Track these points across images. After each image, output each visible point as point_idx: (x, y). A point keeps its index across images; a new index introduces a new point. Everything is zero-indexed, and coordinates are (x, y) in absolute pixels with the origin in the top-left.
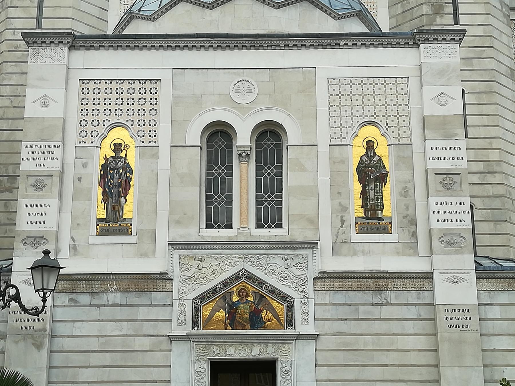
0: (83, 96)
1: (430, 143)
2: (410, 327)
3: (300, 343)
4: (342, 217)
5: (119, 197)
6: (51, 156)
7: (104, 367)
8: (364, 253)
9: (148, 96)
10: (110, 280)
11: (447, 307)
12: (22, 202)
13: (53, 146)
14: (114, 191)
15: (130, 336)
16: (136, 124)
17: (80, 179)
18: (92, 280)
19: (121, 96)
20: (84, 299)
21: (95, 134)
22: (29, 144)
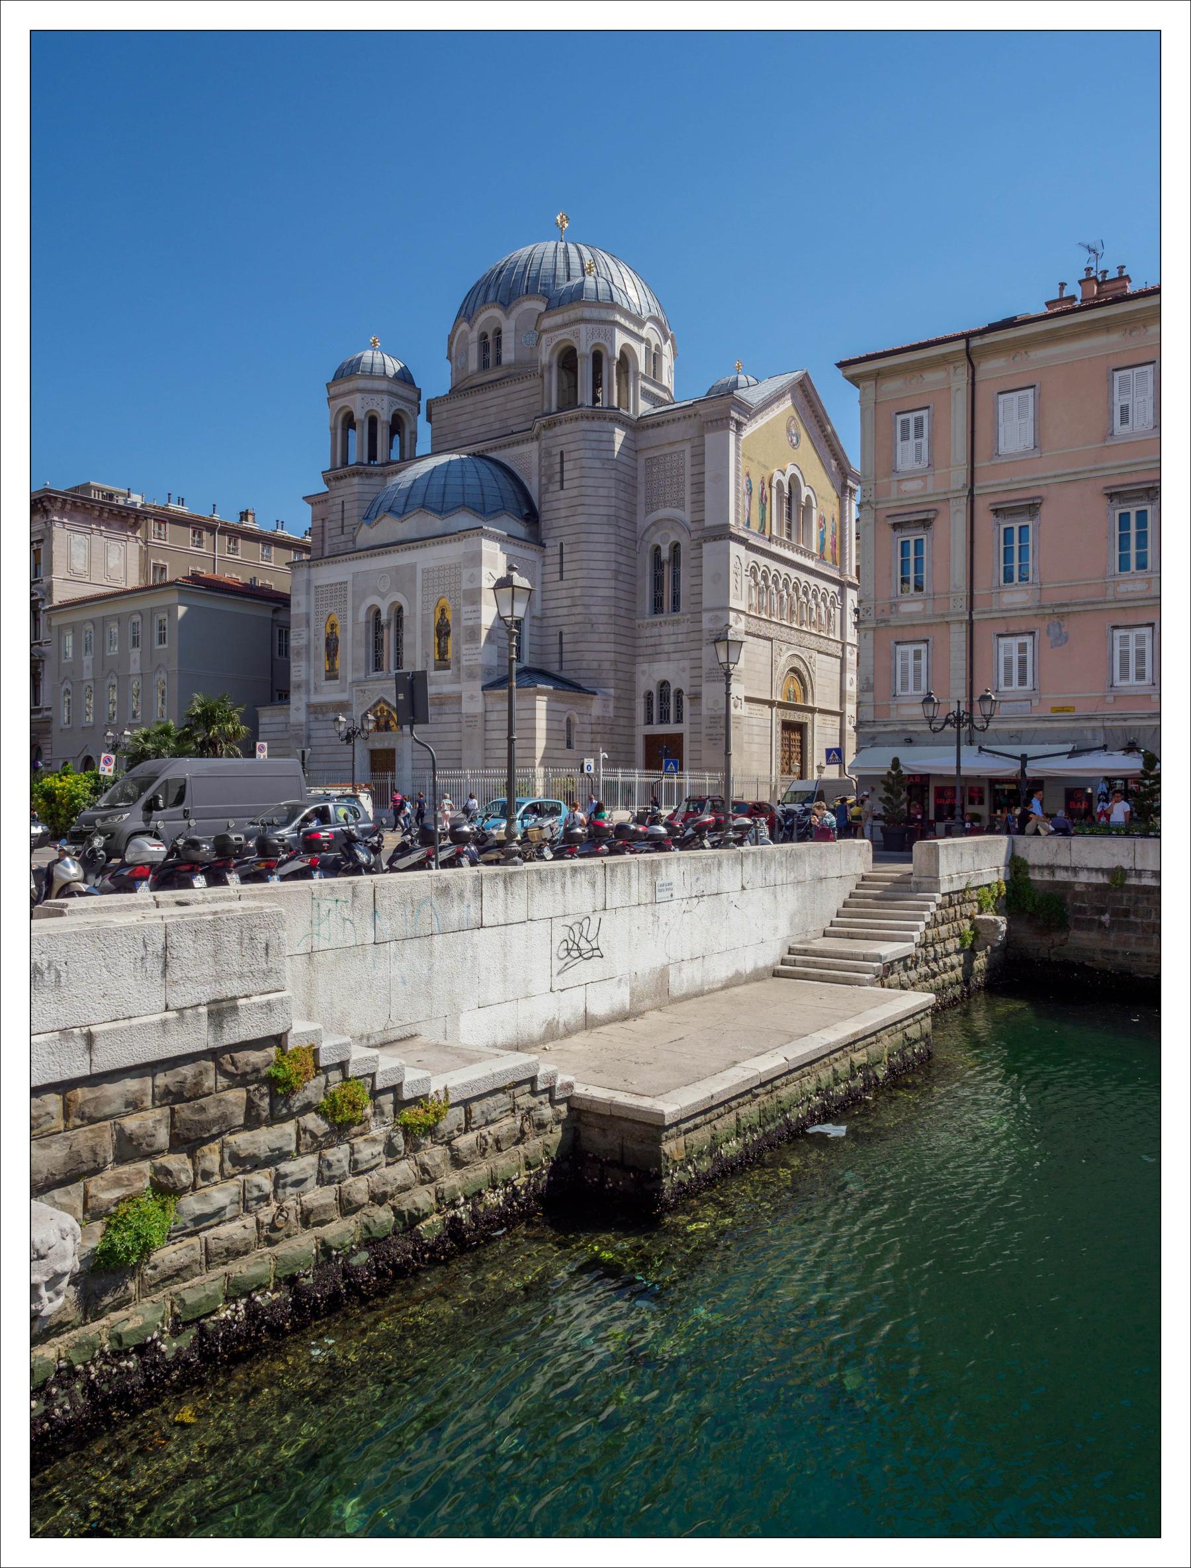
20: (320, 717)
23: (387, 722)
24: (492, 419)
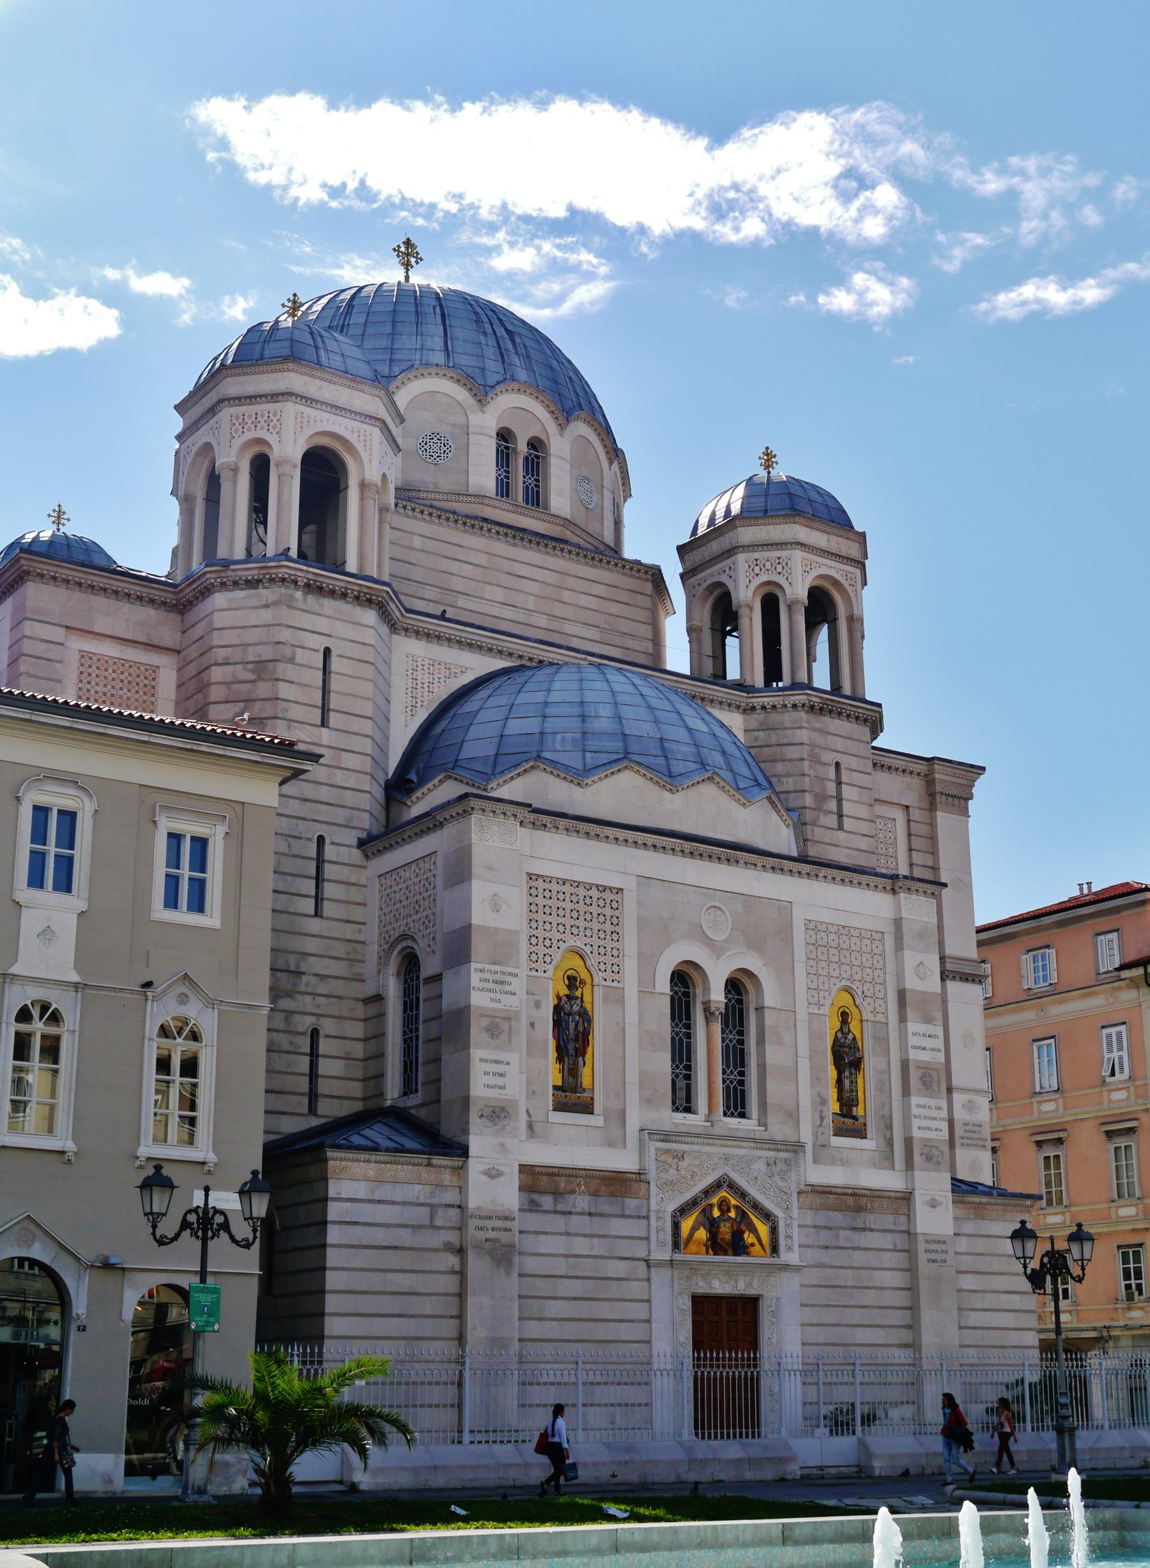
0: (531, 899)
1: (913, 1026)
2: (888, 1259)
3: (785, 1276)
4: (821, 1111)
5: (577, 1056)
6: (507, 988)
7: (575, 1299)
8: (844, 1163)
9: (608, 912)
10: (576, 1176)
11: (928, 1238)
12: (476, 1054)
13: (510, 974)
14: (571, 1046)
15: (602, 1257)
16: (596, 952)
17: (532, 1025)
18: (558, 1175)
19: (577, 906)
20: (547, 1201)
21: (548, 959)
22: (480, 966)
23: (738, 1235)
24: (531, 603)
